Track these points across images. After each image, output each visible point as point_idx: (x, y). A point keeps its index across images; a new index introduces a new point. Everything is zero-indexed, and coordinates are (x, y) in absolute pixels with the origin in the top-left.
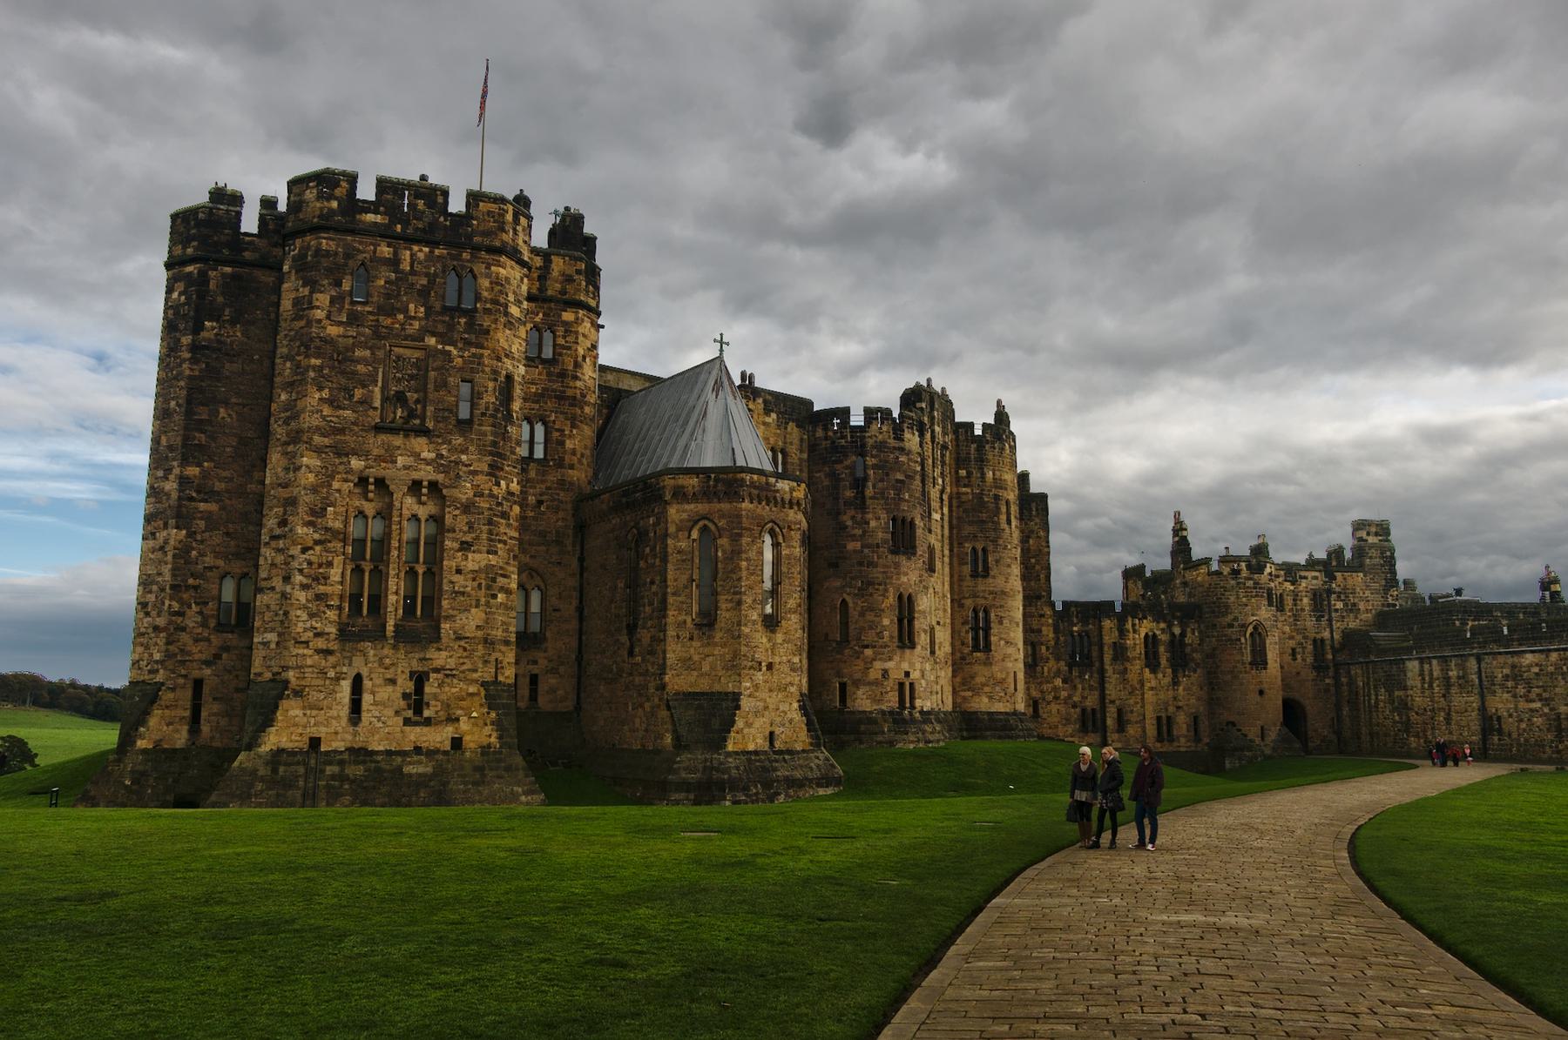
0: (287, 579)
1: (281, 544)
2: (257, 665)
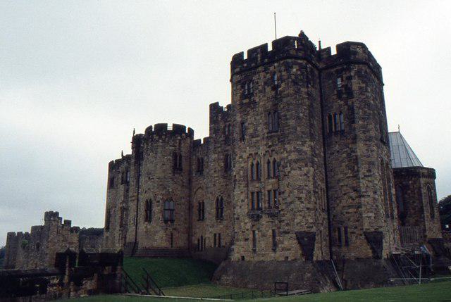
0: (375, 193)
1: (370, 179)
2: (366, 226)
